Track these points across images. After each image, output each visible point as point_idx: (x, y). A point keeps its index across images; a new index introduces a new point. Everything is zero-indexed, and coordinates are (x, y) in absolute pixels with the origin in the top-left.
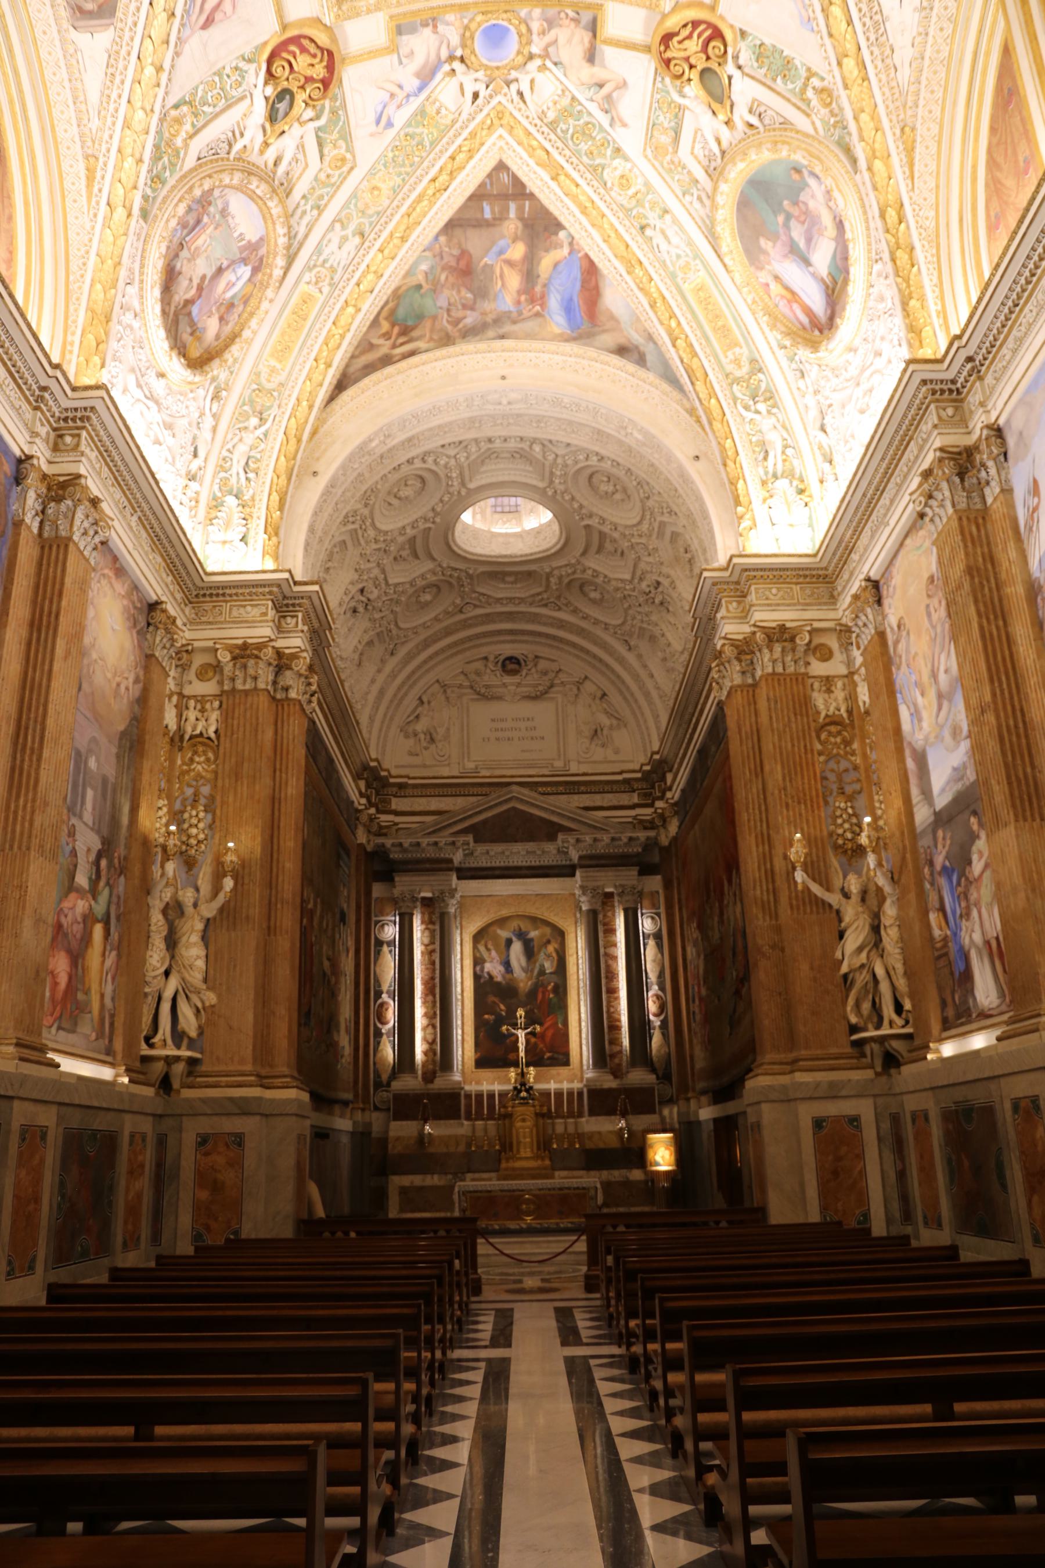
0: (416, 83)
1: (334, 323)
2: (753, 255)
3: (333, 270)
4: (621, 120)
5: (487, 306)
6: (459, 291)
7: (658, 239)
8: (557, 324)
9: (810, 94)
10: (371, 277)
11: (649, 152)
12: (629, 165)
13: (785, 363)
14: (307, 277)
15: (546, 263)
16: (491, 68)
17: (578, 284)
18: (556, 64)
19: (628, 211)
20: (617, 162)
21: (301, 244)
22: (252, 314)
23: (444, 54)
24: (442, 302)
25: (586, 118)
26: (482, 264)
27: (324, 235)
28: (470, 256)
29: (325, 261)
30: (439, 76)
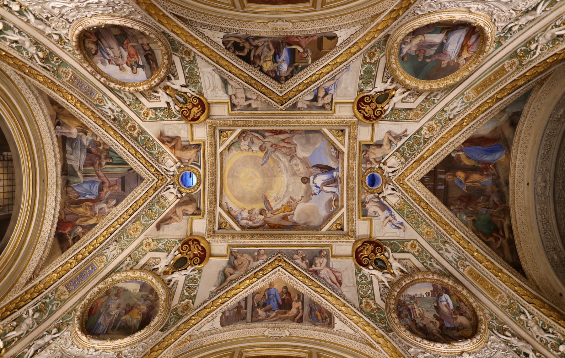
0: (386, 212)
1: (481, 263)
2: (453, 68)
3: (459, 258)
4: (404, 132)
5: (488, 190)
6: (479, 203)
7: (455, 112)
8: (500, 157)
9: (373, 61)
10: (462, 242)
11: (417, 120)
12: (424, 128)
13: (508, 41)
14: (461, 270)
15: (467, 162)
16: (383, 183)
17: (478, 147)
18: (383, 159)
19: (443, 126)
20: (422, 132)
21: (446, 269)
22: (467, 300)
23: (376, 200)
24: (484, 211)
25: (405, 147)
26: (466, 191)
27: (445, 259)
28: (461, 196)
29: (455, 260)
30: (385, 202)
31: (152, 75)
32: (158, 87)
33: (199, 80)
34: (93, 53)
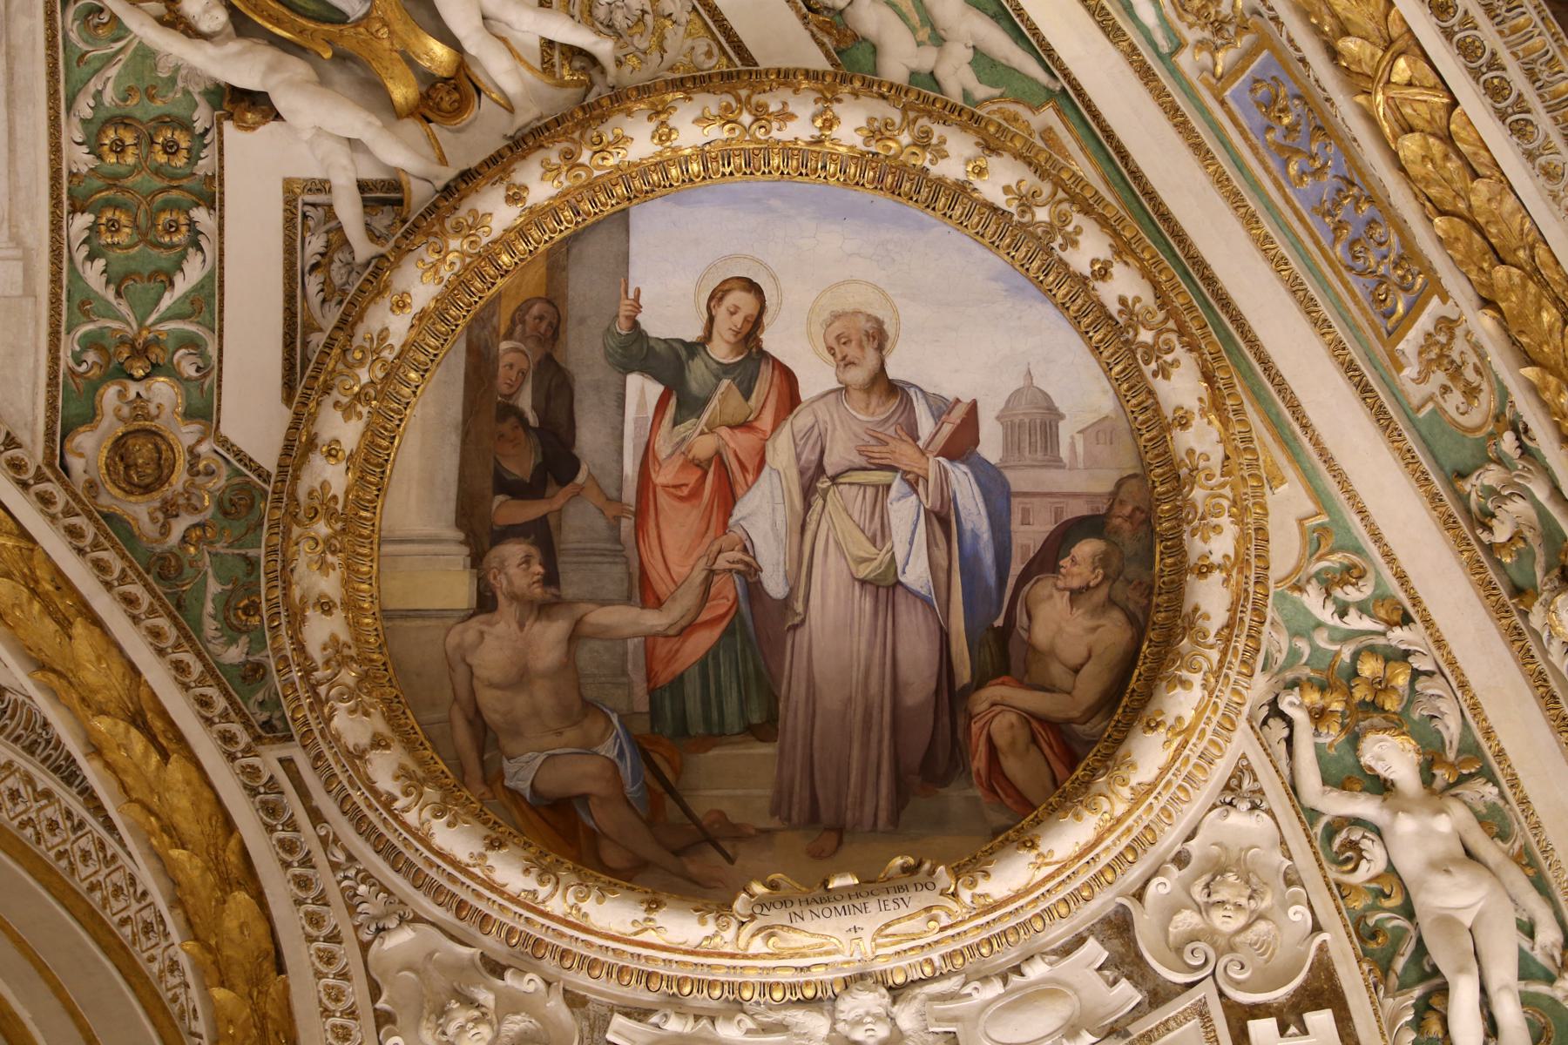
31: (558, 260)
32: (527, 115)
33: (79, 158)
34: (1086, 549)
